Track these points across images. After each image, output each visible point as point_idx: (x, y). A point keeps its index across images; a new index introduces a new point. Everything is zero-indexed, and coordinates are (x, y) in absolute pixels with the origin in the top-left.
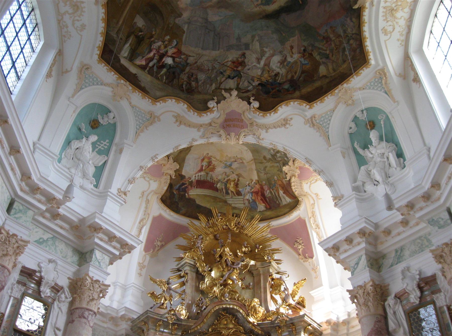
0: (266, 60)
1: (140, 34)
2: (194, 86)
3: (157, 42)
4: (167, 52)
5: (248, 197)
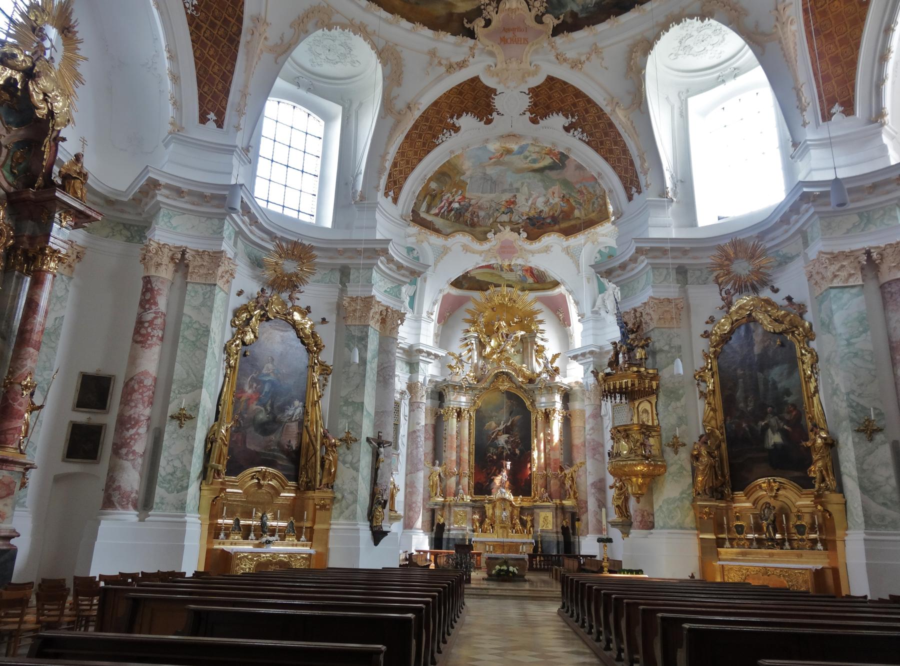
5: (520, 273)
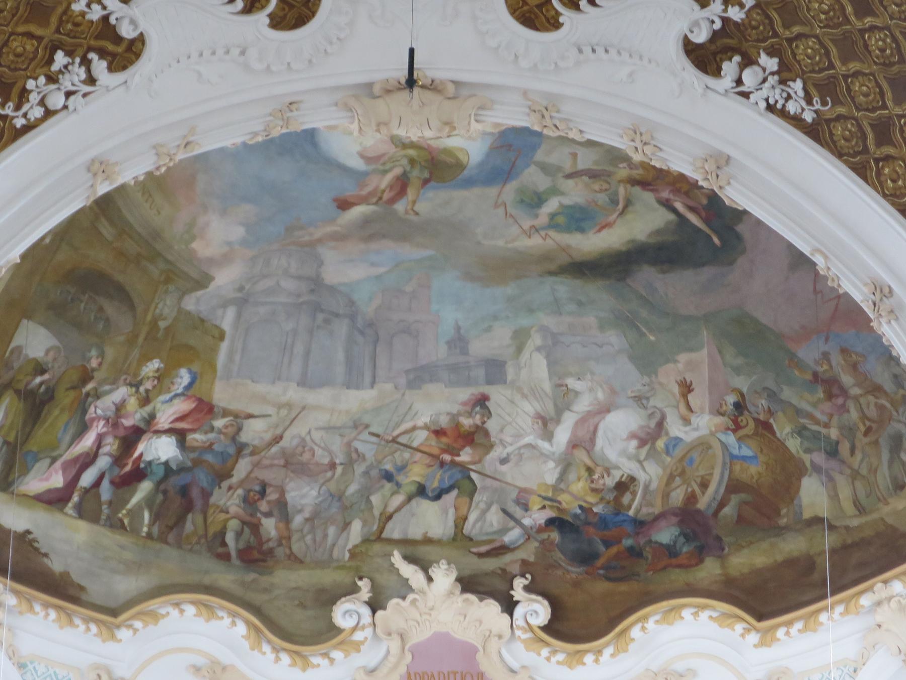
0: (577, 424)
1: (38, 380)
2: (273, 533)
3: (110, 392)
4: (152, 417)
